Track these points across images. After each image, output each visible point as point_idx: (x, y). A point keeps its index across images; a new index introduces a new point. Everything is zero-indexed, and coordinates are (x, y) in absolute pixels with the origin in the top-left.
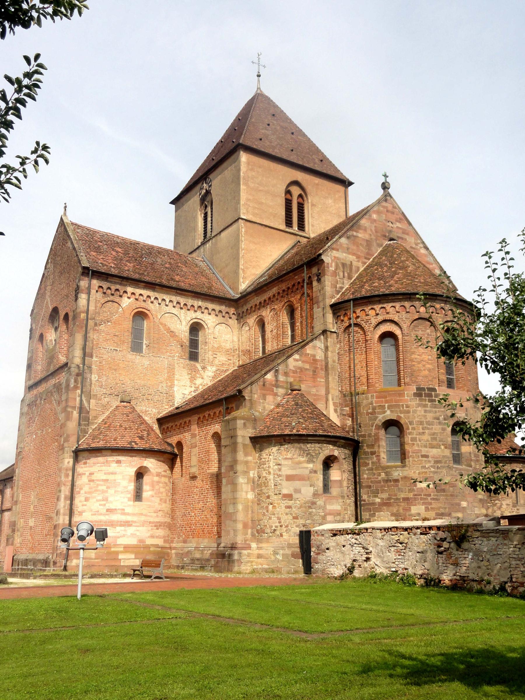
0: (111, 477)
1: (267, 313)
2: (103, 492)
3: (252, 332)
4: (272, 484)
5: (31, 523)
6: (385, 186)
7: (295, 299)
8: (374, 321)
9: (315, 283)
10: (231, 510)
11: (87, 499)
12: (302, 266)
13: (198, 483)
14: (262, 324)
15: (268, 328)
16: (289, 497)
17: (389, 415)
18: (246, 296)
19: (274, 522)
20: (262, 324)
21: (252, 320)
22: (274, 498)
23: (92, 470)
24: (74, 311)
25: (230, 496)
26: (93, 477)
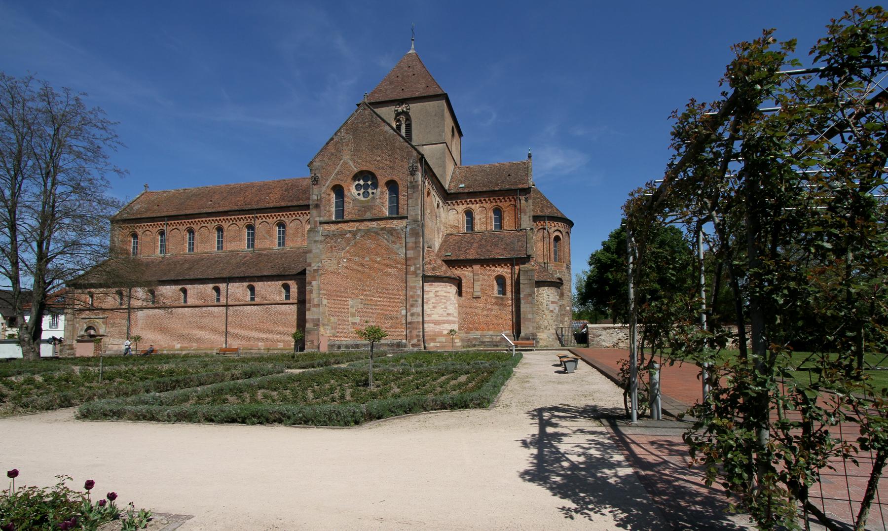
0: (448, 295)
1: (476, 208)
2: (445, 303)
3: (460, 216)
4: (545, 305)
5: (357, 320)
6: (530, 156)
7: (504, 204)
8: (553, 229)
9: (523, 202)
10: (530, 316)
11: (434, 307)
12: (516, 190)
13: (482, 301)
14: (469, 214)
15: (478, 217)
16: (552, 311)
17: (558, 275)
18: (451, 194)
19: (546, 323)
20: (469, 214)
21: (461, 208)
22: (547, 312)
23: (437, 289)
24: (411, 182)
25: (529, 309)
26: (438, 294)
